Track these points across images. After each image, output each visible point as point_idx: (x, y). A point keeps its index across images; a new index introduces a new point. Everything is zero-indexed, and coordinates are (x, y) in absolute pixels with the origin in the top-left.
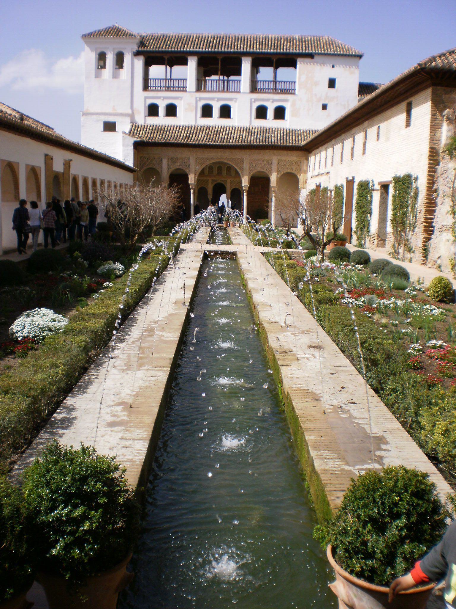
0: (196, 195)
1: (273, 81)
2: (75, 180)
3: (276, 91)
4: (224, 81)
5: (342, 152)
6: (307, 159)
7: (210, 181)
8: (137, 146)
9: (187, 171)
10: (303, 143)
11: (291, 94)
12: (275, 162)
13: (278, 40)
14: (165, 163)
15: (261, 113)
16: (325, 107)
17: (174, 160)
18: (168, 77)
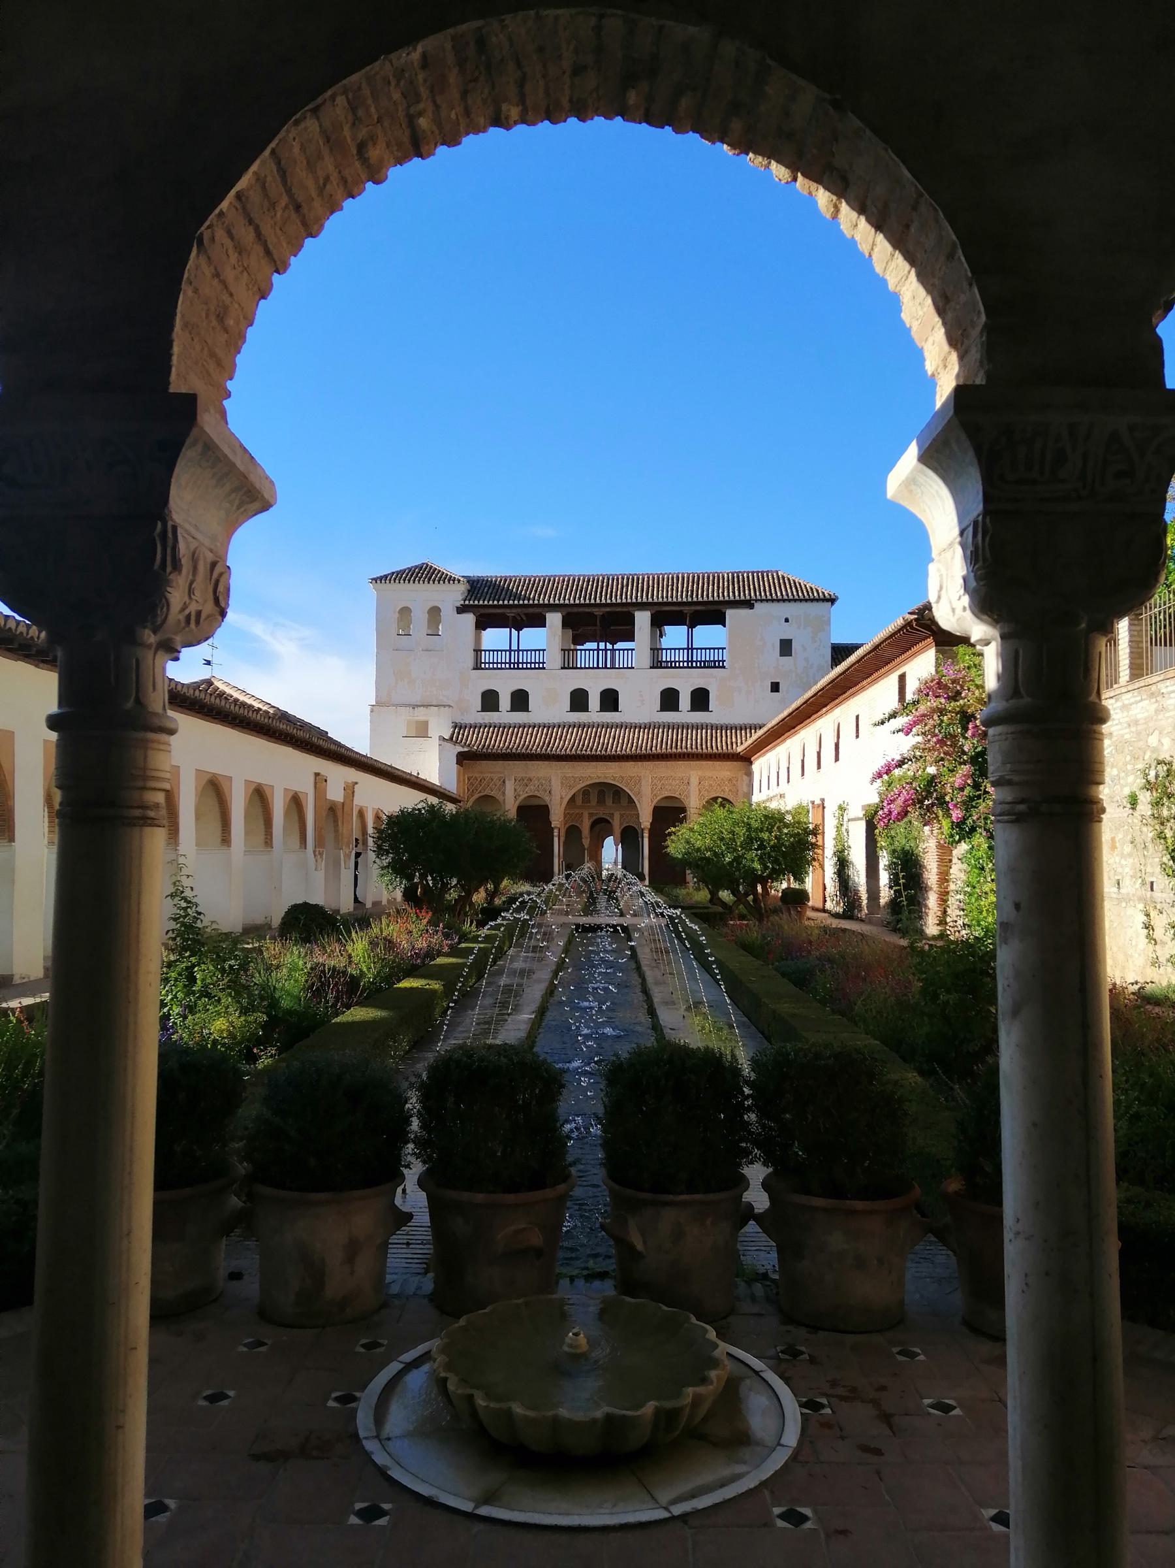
0: (562, 839)
1: (688, 649)
2: (361, 814)
3: (691, 664)
4: (606, 650)
5: (803, 761)
6: (750, 774)
7: (586, 815)
8: (463, 758)
9: (547, 798)
10: (740, 749)
11: (719, 667)
12: (694, 781)
13: (696, 579)
14: (510, 786)
15: (669, 699)
16: (775, 687)
17: (525, 782)
18: (514, 647)
